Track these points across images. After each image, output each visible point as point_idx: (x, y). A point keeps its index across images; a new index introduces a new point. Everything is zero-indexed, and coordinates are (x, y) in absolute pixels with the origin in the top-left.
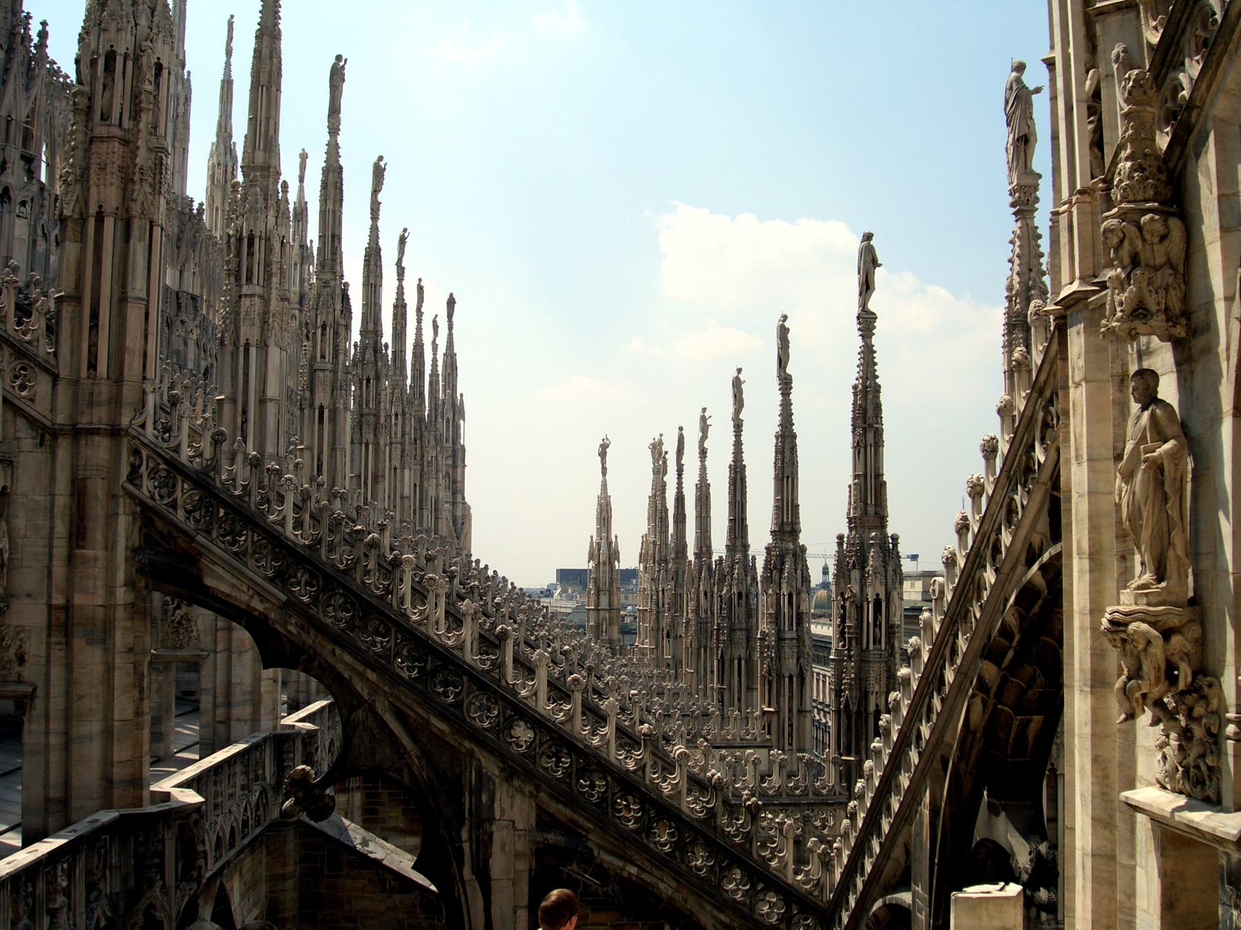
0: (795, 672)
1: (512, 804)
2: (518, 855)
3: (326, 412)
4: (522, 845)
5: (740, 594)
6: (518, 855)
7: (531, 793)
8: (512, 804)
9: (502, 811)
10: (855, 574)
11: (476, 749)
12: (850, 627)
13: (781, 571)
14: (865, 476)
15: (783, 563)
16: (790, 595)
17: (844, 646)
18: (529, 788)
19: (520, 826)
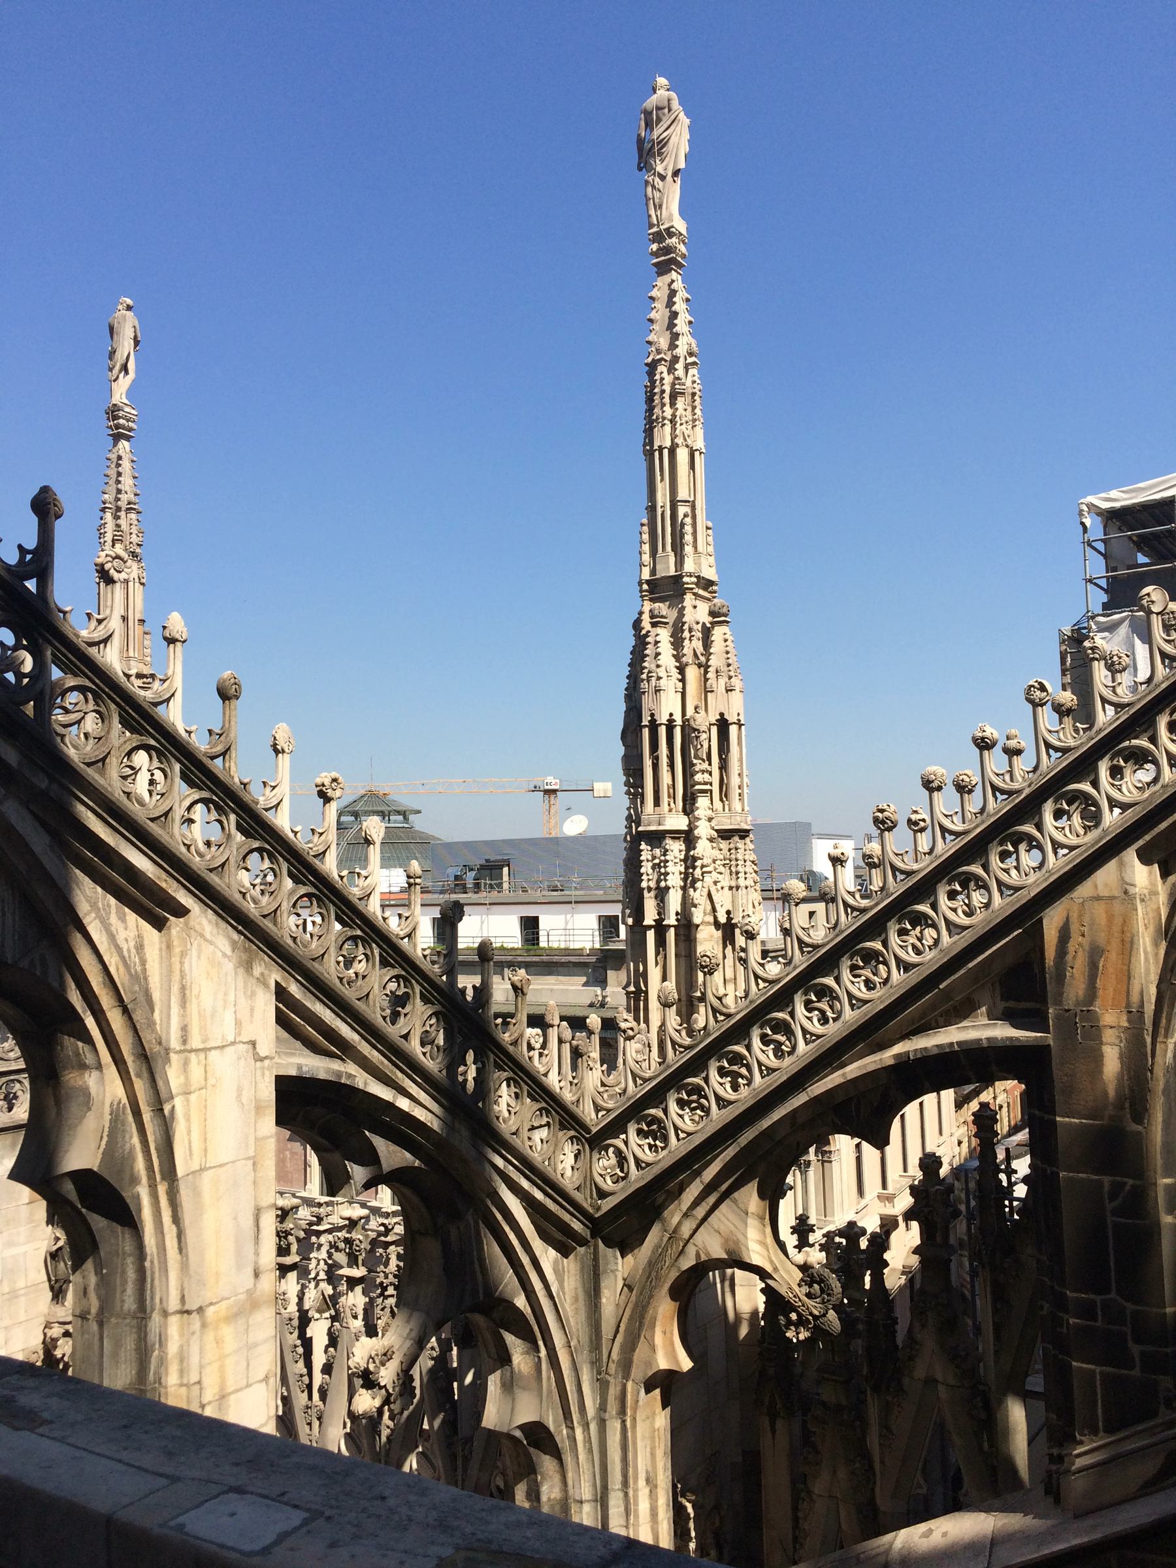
1: (252, 1010)
8: (252, 1010)
9: (238, 1023)
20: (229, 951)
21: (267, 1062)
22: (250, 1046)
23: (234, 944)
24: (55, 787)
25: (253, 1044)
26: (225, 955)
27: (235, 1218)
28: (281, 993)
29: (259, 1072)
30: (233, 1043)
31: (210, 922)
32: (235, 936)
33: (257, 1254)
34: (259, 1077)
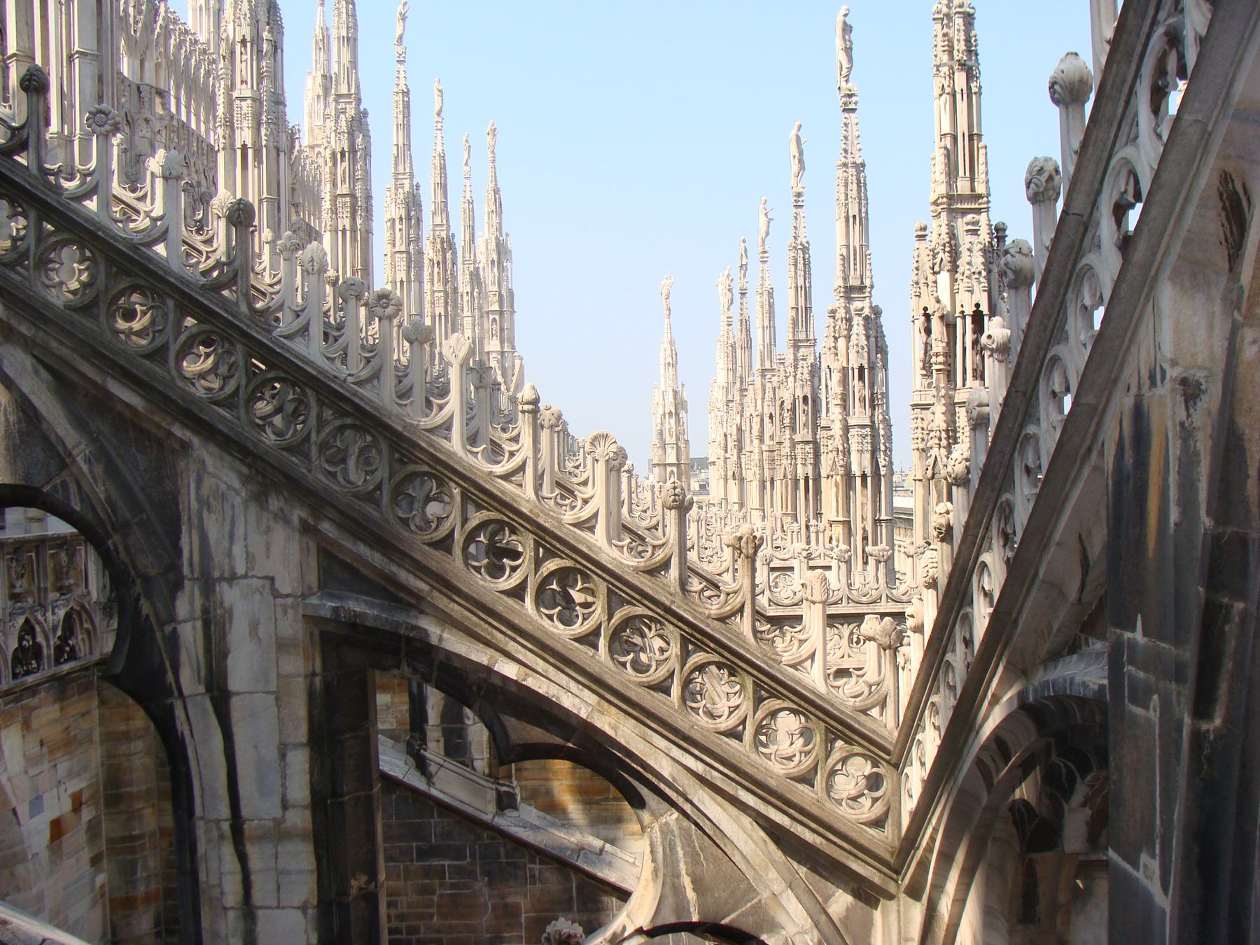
0: (868, 471)
1: (268, 546)
2: (282, 646)
3: (250, 152)
4: (292, 626)
5: (805, 398)
6: (282, 646)
7: (303, 522)
8: (268, 546)
9: (250, 558)
10: (944, 278)
11: (196, 441)
12: (937, 355)
13: (848, 338)
14: (955, 138)
15: (850, 329)
16: (861, 369)
17: (929, 385)
18: (298, 514)
19: (285, 588)
20: (236, 484)
21: (290, 600)
22: (267, 583)
23: (245, 480)
24: (41, 334)
25: (272, 579)
26: (230, 487)
27: (256, 747)
28: (307, 529)
29: (279, 610)
30: (246, 576)
31: (212, 455)
32: (245, 470)
33: (284, 786)
34: (279, 615)
